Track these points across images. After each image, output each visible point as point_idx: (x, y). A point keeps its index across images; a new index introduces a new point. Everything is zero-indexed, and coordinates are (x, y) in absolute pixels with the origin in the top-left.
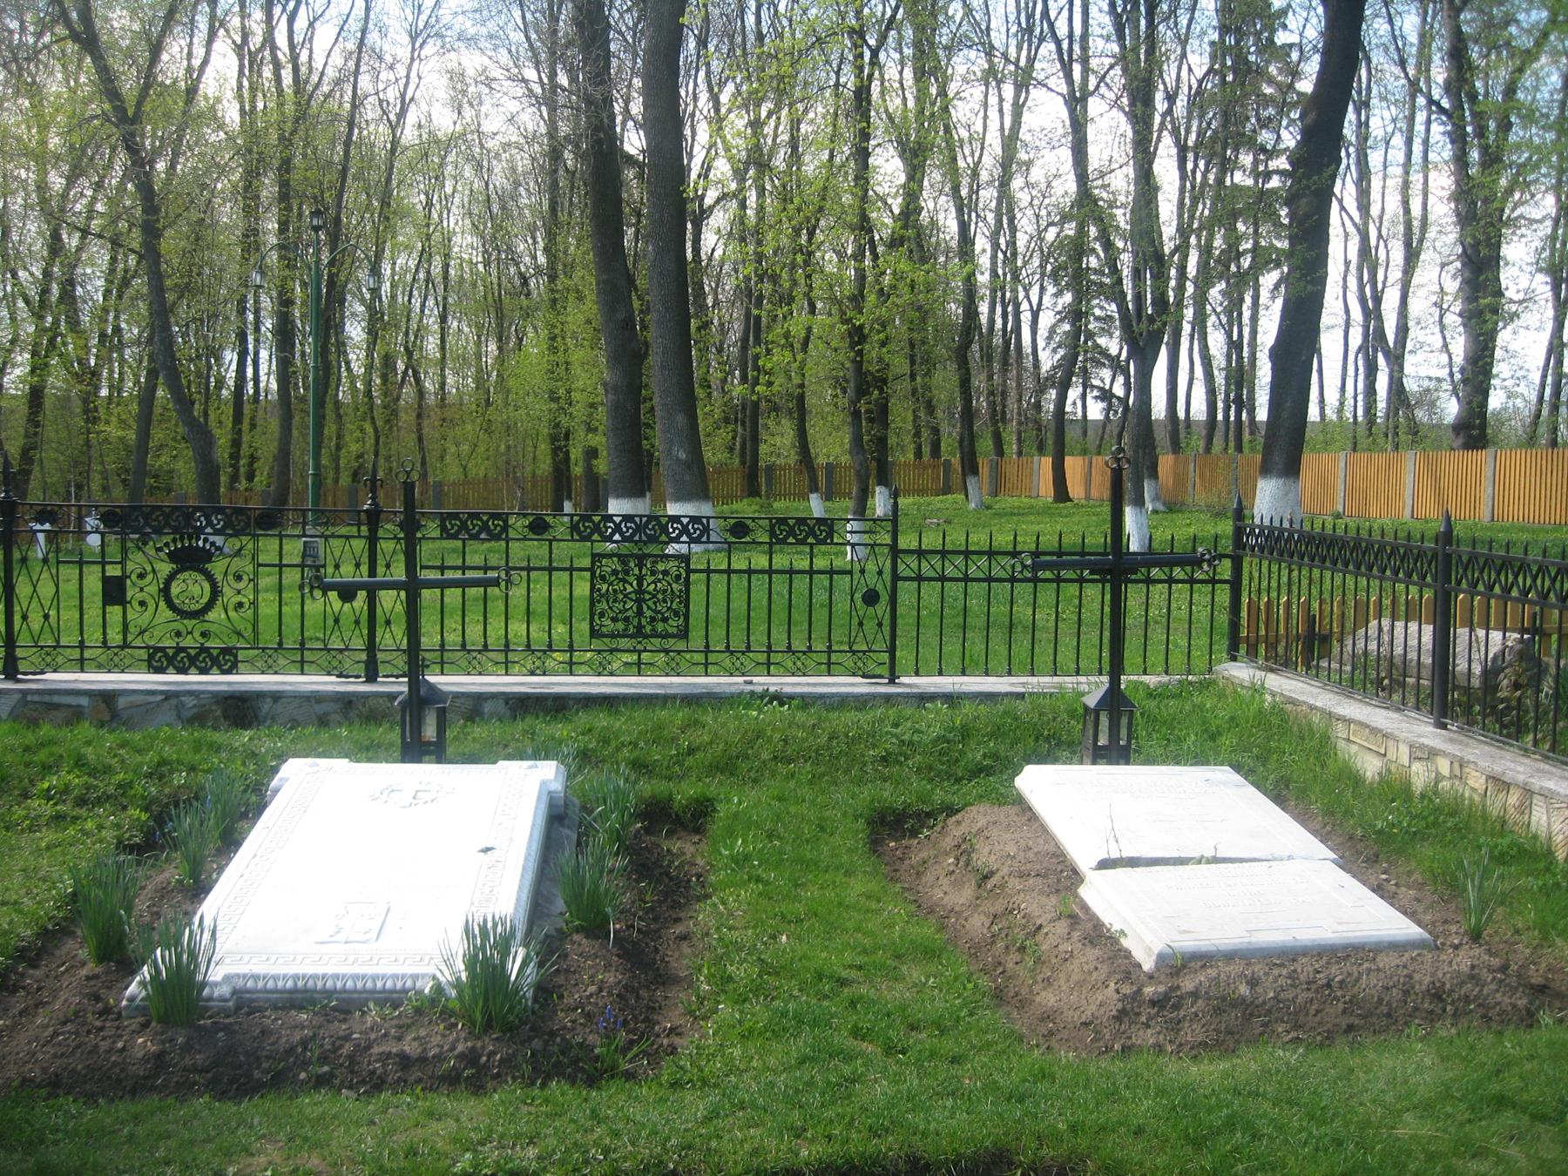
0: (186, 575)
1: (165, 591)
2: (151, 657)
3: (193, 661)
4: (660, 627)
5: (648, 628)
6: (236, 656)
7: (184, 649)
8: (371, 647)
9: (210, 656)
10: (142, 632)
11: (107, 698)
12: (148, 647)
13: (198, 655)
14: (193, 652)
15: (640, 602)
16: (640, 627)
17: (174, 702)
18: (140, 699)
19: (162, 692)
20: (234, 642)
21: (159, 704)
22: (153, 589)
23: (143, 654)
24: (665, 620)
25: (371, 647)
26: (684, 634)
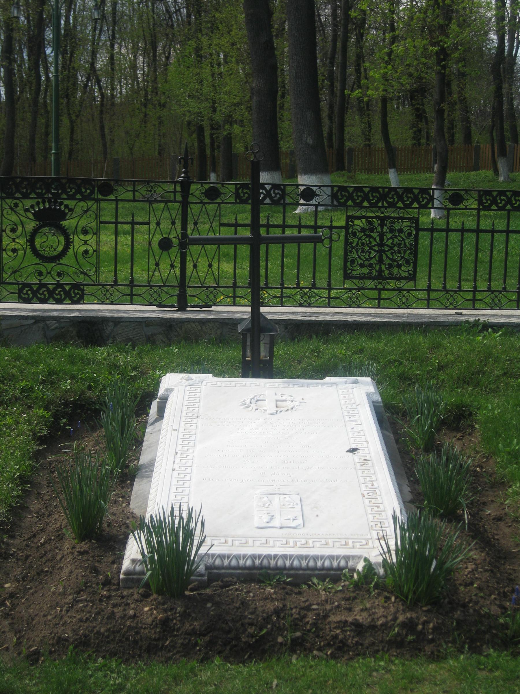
0: (46, 229)
2: (20, 291)
3: (51, 293)
5: (386, 272)
6: (83, 290)
7: (45, 285)
9: (64, 290)
10: (14, 272)
12: (18, 284)
13: (55, 289)
14: (51, 287)
16: (380, 271)
20: (80, 279)
23: (15, 288)
24: (399, 266)
26: (412, 277)
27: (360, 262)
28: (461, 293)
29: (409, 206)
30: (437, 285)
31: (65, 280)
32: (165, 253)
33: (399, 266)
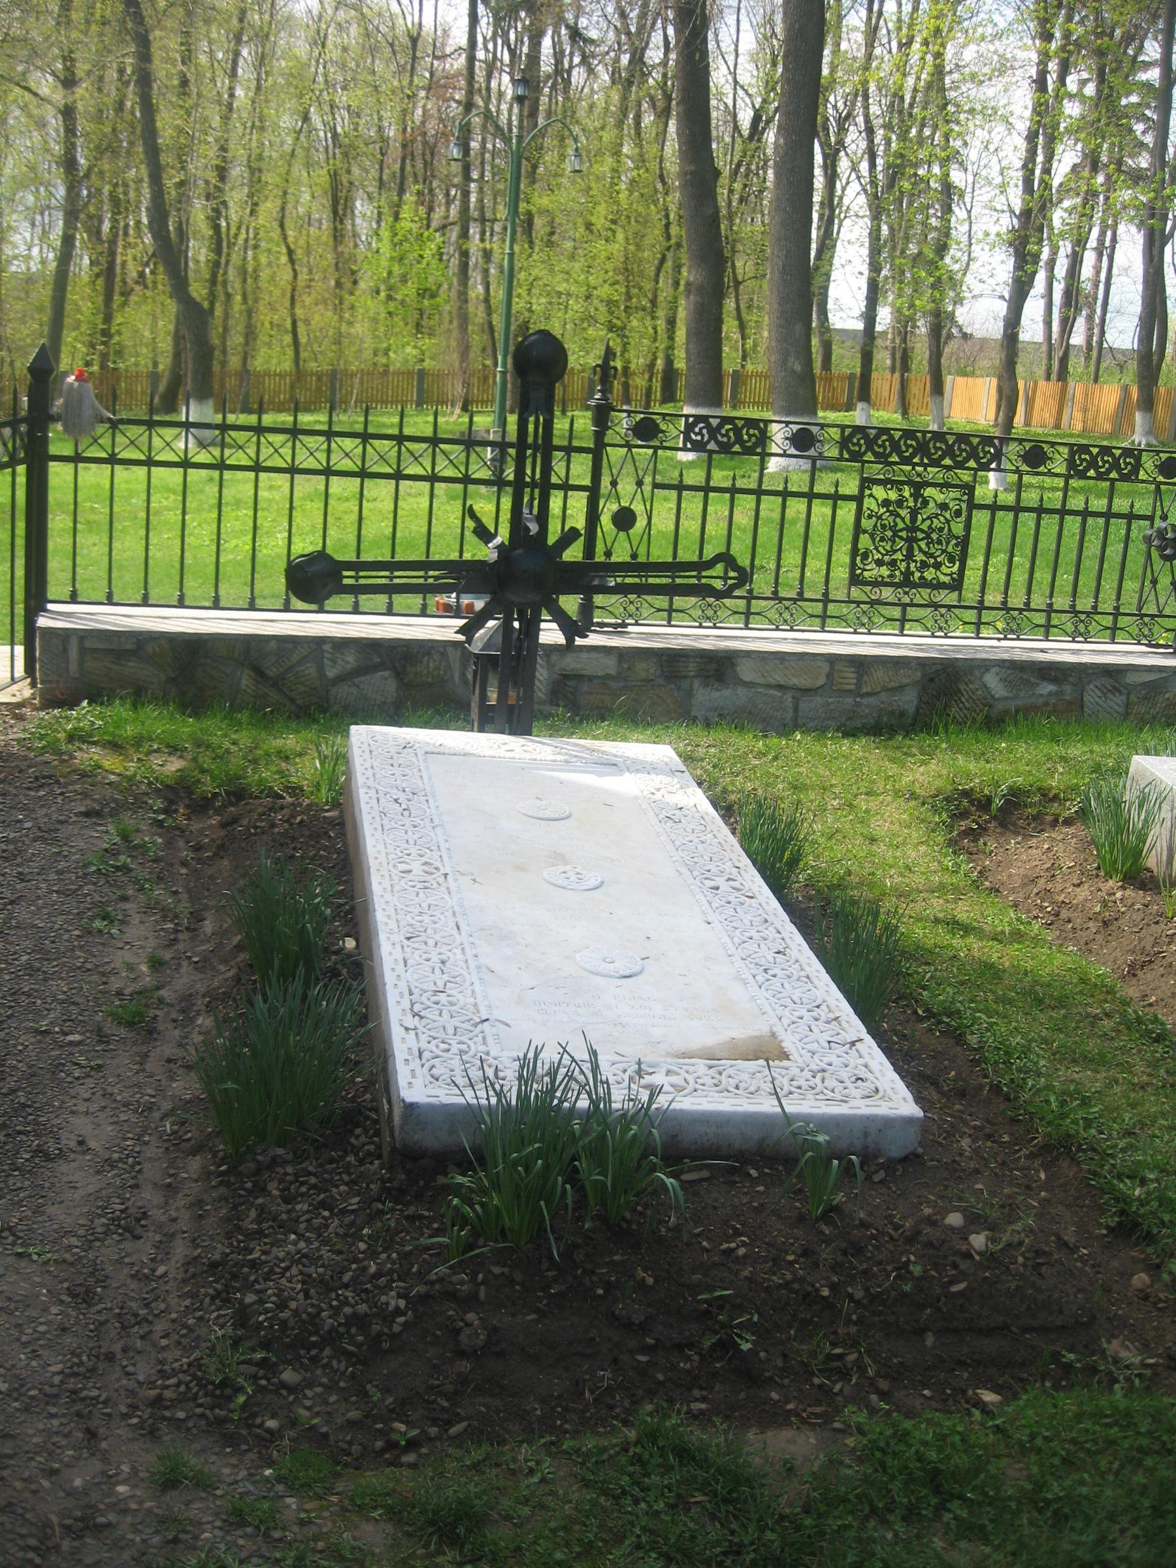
15: (911, 541)
24: (937, 566)
26: (956, 585)
29: (961, 465)
33: (937, 566)
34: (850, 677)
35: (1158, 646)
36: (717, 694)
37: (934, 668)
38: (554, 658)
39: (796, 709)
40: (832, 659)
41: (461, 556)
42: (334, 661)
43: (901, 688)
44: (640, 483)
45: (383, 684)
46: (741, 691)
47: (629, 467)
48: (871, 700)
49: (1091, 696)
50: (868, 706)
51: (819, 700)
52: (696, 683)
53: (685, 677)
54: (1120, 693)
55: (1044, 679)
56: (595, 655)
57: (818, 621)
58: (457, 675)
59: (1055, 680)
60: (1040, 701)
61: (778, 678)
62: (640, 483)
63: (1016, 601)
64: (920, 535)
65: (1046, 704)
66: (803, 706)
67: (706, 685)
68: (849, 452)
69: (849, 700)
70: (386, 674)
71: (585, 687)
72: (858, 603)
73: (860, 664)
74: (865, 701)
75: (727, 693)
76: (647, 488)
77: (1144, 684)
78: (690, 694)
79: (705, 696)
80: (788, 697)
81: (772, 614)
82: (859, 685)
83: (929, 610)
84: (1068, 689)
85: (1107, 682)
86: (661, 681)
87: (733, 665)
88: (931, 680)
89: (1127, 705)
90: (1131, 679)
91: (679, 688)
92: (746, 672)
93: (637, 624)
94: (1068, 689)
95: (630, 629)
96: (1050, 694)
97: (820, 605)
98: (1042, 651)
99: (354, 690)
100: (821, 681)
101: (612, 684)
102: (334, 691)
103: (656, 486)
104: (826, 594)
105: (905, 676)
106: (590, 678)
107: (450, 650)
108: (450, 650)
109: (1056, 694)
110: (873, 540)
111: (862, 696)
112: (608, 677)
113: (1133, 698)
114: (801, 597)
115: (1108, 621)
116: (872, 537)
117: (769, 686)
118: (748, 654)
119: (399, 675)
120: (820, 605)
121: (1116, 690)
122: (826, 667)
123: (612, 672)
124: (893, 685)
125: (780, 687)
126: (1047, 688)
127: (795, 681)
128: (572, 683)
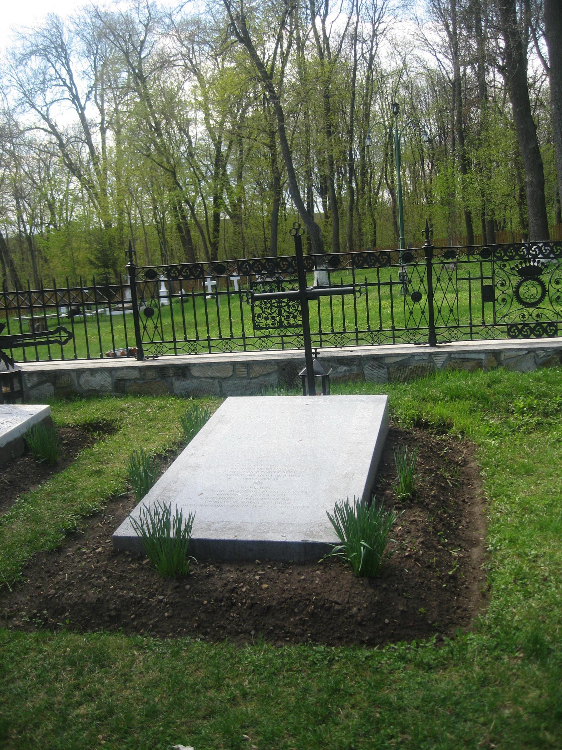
1: (517, 292)
2: (509, 330)
3: (532, 331)
4: (292, 321)
5: (286, 322)
6: (556, 327)
7: (527, 325)
8: (432, 327)
9: (542, 327)
10: (504, 316)
11: (496, 354)
12: (507, 325)
13: (535, 327)
14: (532, 326)
16: (281, 322)
17: (532, 354)
18: (514, 354)
19: (526, 349)
21: (524, 356)
22: (510, 291)
23: (505, 328)
25: (432, 327)
27: (264, 315)
28: (347, 335)
30: (214, 335)
31: (543, 320)
32: (149, 319)
34: (74, 375)
35: (419, 344)
36: (184, 383)
37: (284, 364)
38: (113, 373)
39: (221, 387)
40: (234, 364)
41: (300, 326)
42: (29, 380)
43: (269, 374)
44: (450, 279)
45: (48, 388)
46: (194, 381)
47: (416, 274)
48: (256, 380)
49: (367, 371)
50: (254, 383)
51: (231, 382)
52: (174, 379)
53: (169, 377)
54: (383, 368)
55: (341, 365)
56: (129, 370)
57: (355, 342)
58: (76, 382)
59: (345, 365)
60: (341, 375)
61: (210, 374)
62: (450, 279)
63: (375, 327)
64: (276, 305)
65: (345, 376)
66: (224, 385)
67: (178, 380)
68: (243, 272)
69: (245, 381)
70: (49, 384)
71: (128, 384)
72: (260, 338)
73: (247, 364)
74: (253, 381)
75: (188, 382)
76: (454, 281)
77: (396, 362)
78: (172, 384)
79: (179, 385)
80: (216, 382)
81: (220, 346)
82: (248, 373)
83: (295, 337)
84: (355, 368)
85: (375, 363)
86: (158, 379)
87: (189, 370)
88: (283, 369)
89: (389, 374)
90: (387, 361)
91: (167, 382)
92: (195, 372)
93: (162, 356)
94: (355, 368)
95: (159, 358)
96: (345, 371)
97: (207, 342)
98: (351, 351)
99: (38, 391)
100: (230, 374)
101: (139, 382)
102: (31, 392)
103: (457, 279)
104: (244, 335)
105: (268, 369)
106: (130, 380)
107: (72, 373)
108: (72, 373)
109: (348, 371)
110: (262, 309)
111: (251, 379)
112: (136, 379)
113: (391, 370)
114: (345, 331)
115: (390, 334)
116: (261, 307)
117: (207, 378)
118: (194, 365)
119: (54, 384)
120: (207, 342)
121: (380, 367)
122: (231, 368)
123: (138, 376)
124: (265, 373)
125: (211, 378)
126: (343, 368)
127: (218, 375)
128: (123, 383)
